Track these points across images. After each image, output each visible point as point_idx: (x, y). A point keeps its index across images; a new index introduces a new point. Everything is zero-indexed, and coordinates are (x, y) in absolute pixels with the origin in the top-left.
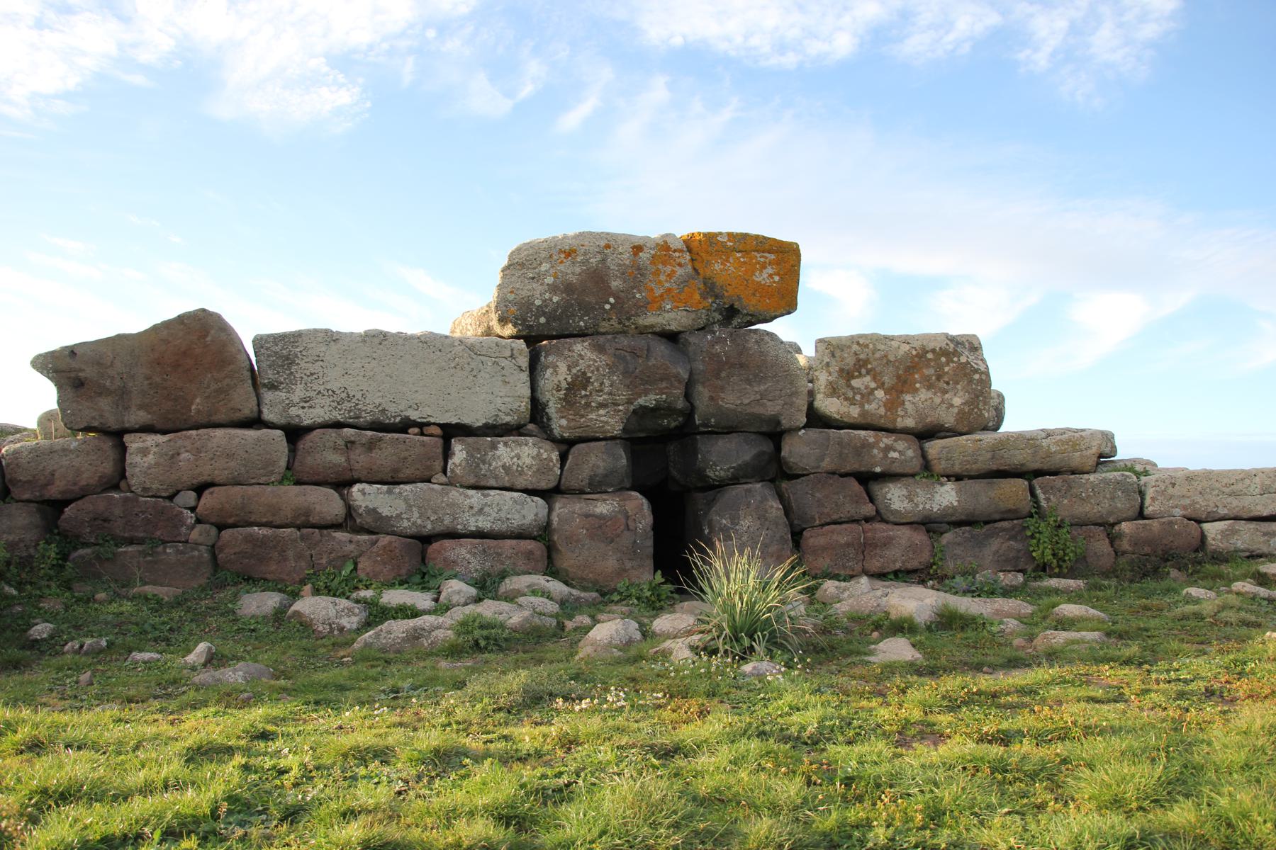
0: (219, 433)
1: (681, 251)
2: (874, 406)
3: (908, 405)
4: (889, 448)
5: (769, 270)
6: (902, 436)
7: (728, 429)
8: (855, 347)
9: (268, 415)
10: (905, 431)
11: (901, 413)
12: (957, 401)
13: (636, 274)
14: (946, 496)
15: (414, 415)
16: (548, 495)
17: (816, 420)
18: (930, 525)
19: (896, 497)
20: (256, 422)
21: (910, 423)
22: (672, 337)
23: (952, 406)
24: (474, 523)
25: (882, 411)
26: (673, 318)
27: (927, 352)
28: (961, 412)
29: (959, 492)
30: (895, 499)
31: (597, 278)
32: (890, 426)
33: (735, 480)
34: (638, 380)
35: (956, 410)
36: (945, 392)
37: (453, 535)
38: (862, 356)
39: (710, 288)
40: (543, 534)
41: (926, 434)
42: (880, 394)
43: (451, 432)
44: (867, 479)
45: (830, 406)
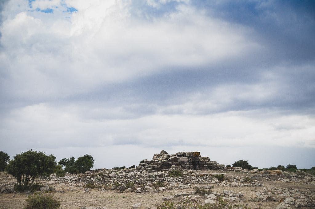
7: (196, 162)
13: (193, 154)
14: (207, 165)
16: (189, 165)
17: (201, 161)
18: (206, 167)
19: (204, 165)
22: (194, 157)
26: (194, 156)
31: (191, 154)
33: (197, 164)
34: (193, 160)
39: (196, 155)
40: (189, 167)
41: (206, 162)
43: (185, 162)
44: (203, 165)
45: (201, 161)
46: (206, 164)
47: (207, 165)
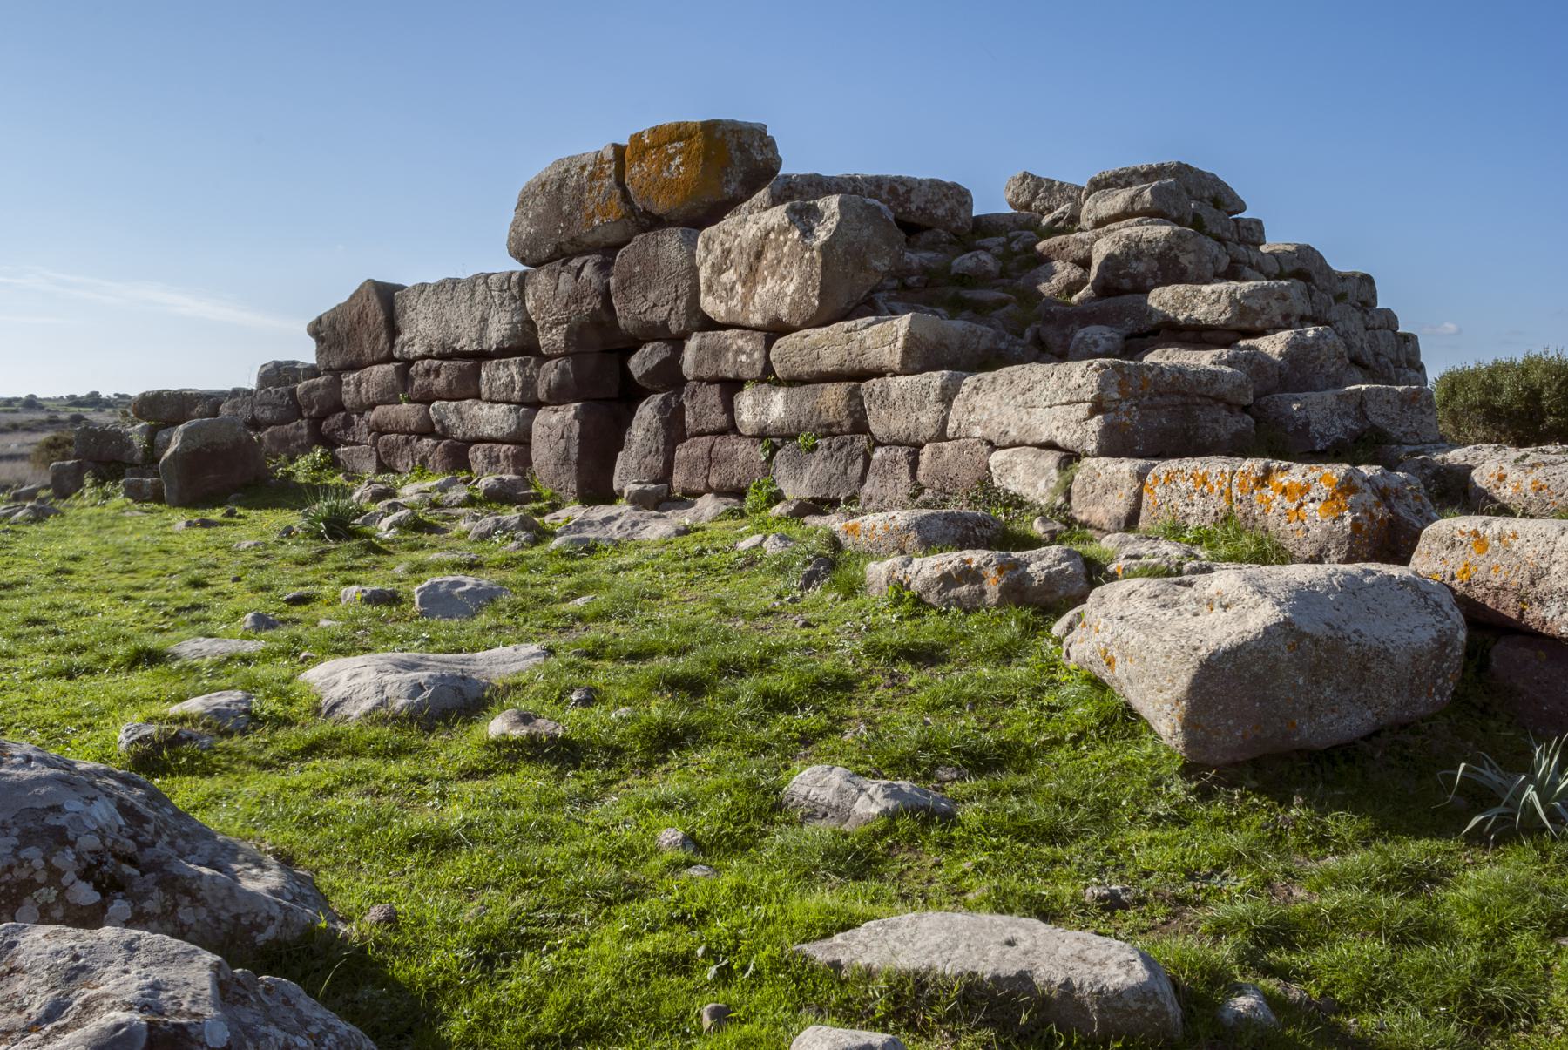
0: (375, 368)
1: (610, 161)
2: (735, 303)
3: (757, 299)
4: (740, 351)
5: (678, 161)
6: (756, 334)
8: (722, 235)
9: (397, 354)
10: (756, 329)
11: (752, 308)
12: (792, 287)
14: (776, 407)
15: (458, 346)
20: (389, 359)
21: (756, 319)
23: (786, 295)
24: (487, 431)
25: (739, 306)
27: (769, 233)
28: (793, 303)
29: (787, 399)
30: (745, 410)
32: (746, 324)
35: (788, 300)
36: (783, 278)
37: (480, 440)
38: (727, 245)
41: (775, 330)
42: (739, 287)
46: (768, 377)
47: (776, 407)
